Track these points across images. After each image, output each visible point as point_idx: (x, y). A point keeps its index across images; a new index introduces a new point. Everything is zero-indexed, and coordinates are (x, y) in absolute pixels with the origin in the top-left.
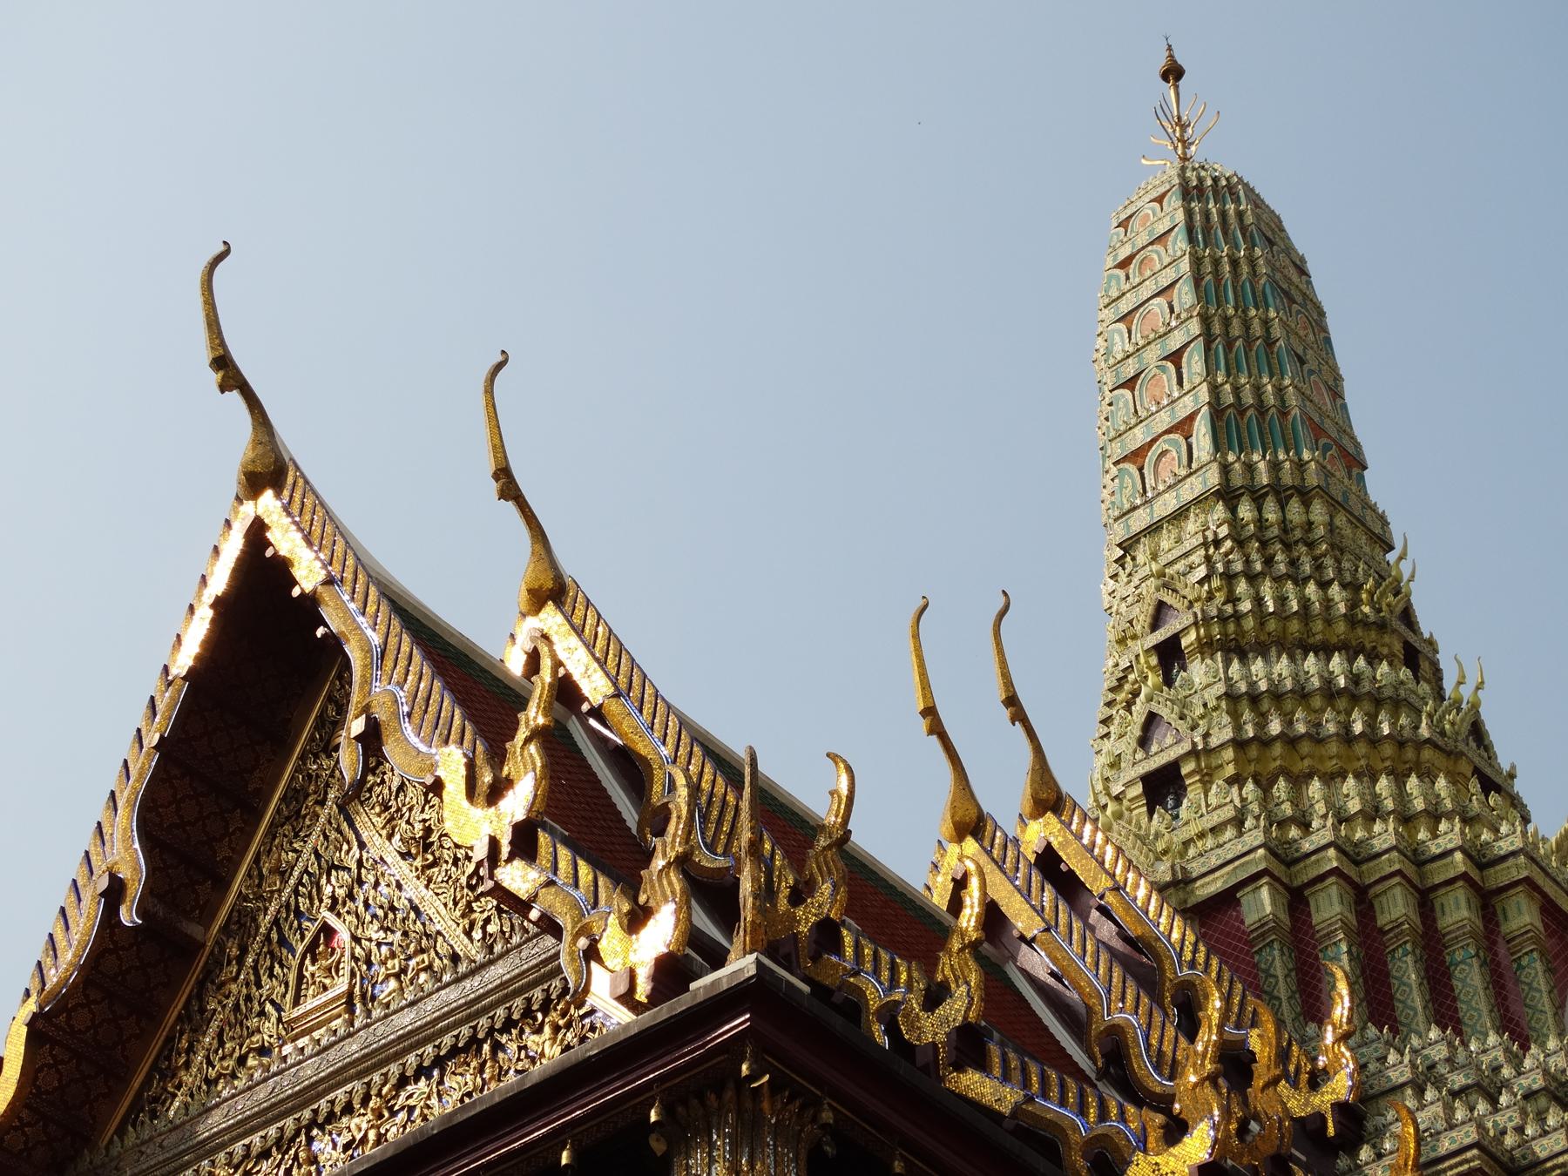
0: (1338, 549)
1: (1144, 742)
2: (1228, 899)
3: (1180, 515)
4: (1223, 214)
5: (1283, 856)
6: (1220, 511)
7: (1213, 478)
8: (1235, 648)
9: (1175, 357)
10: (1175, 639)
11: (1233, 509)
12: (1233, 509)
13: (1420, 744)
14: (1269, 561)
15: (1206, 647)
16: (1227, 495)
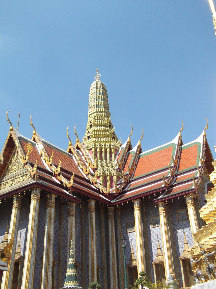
0: (105, 117)
1: (88, 134)
2: (91, 149)
3: (93, 113)
4: (99, 86)
5: (95, 145)
6: (96, 114)
7: (96, 111)
8: (96, 126)
9: (94, 99)
10: (91, 125)
11: (97, 113)
12: (97, 113)
13: (108, 135)
14: (99, 118)
15: (94, 125)
16: (97, 112)
